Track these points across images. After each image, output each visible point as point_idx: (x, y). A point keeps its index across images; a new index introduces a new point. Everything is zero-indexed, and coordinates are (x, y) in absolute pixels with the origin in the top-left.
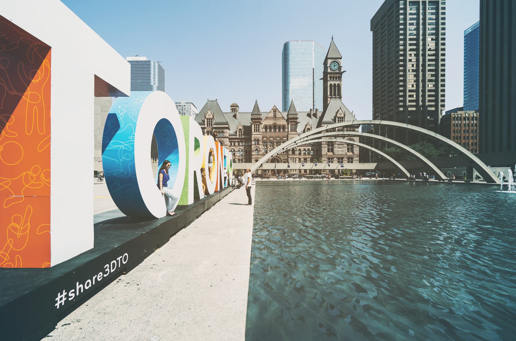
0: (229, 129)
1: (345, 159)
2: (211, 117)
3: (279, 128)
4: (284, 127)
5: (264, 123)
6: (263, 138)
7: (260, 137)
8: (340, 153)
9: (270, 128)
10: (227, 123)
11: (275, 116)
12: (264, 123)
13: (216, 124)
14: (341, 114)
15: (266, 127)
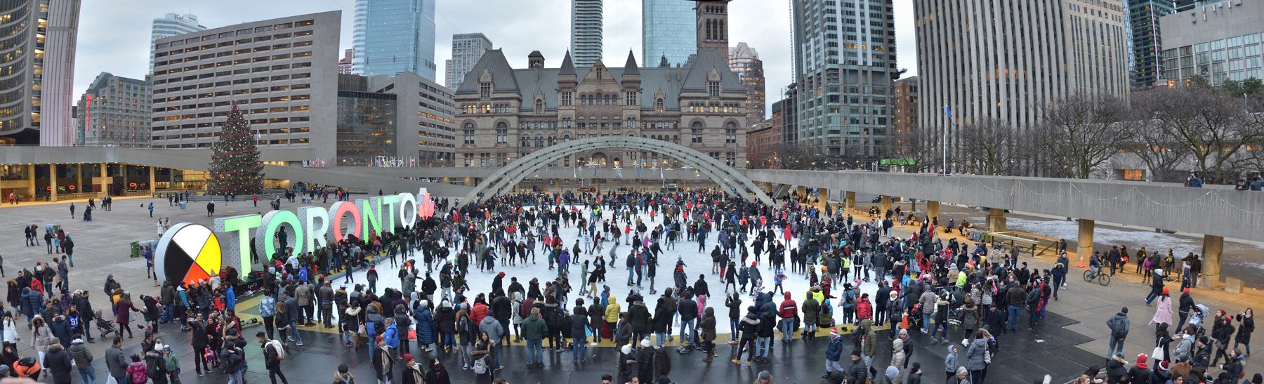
0: (520, 100)
1: (723, 155)
2: (489, 79)
3: (607, 97)
4: (615, 97)
5: (582, 89)
6: (577, 116)
7: (572, 113)
8: (715, 144)
9: (591, 97)
10: (517, 90)
11: (599, 76)
12: (582, 89)
13: (496, 91)
14: (714, 76)
15: (583, 96)
